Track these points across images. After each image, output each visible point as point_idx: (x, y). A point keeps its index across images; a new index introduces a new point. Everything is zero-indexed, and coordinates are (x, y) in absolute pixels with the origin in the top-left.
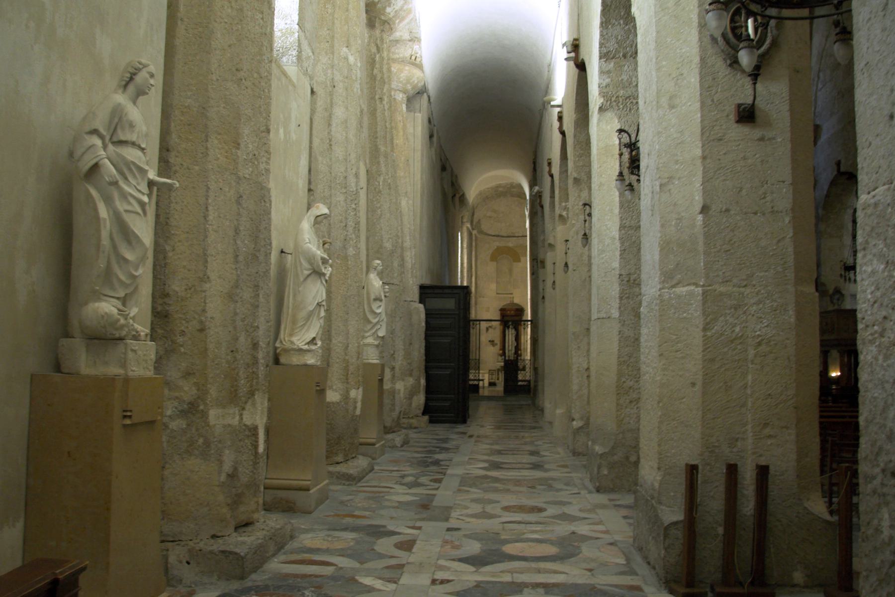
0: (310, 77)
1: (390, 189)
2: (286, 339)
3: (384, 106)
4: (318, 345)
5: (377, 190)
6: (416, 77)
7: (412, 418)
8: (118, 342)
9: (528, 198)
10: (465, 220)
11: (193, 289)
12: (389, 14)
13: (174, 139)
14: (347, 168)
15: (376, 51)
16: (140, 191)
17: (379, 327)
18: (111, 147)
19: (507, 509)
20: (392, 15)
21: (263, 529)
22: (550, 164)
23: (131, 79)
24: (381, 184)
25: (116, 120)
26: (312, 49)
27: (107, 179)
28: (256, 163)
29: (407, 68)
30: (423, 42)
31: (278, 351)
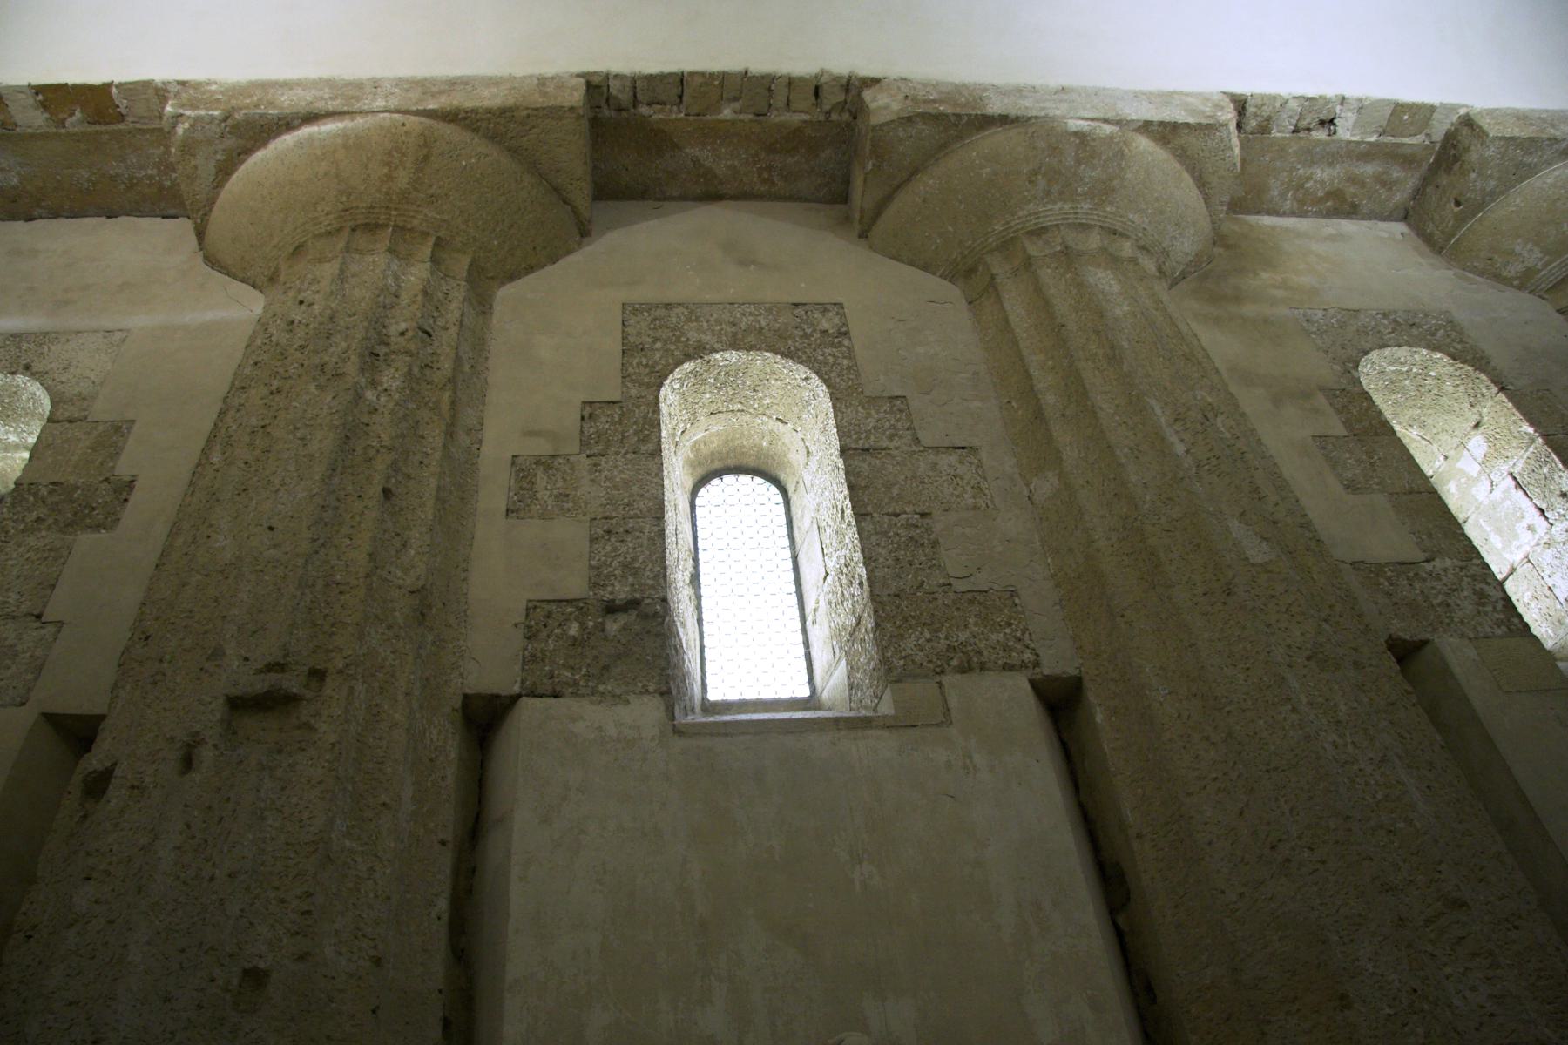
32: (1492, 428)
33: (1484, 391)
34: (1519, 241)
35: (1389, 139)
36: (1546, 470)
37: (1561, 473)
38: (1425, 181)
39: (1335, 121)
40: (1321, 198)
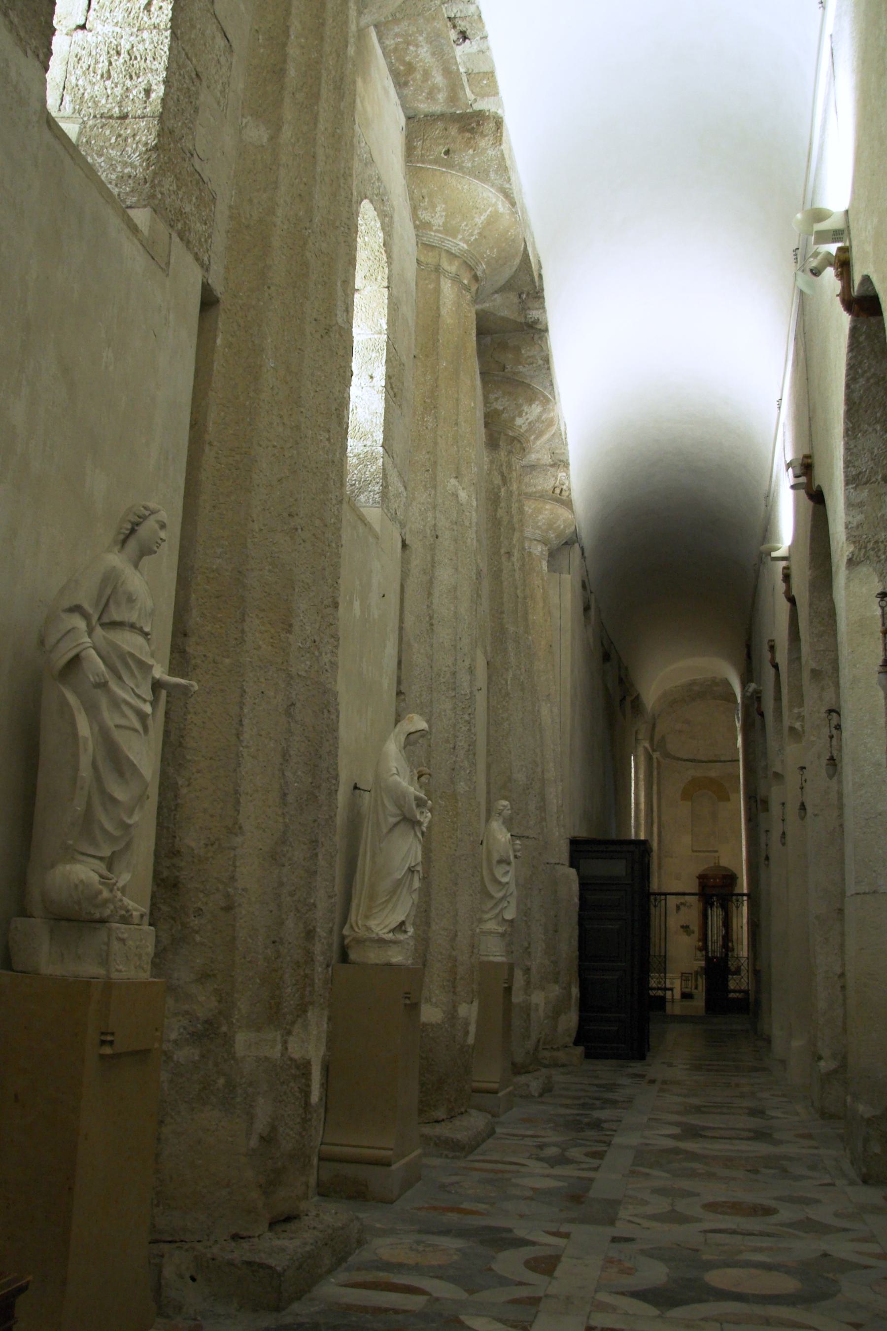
0: (400, 523)
1: (523, 690)
2: (360, 923)
3: (513, 565)
4: (410, 934)
5: (503, 691)
6: (562, 519)
7: (558, 1049)
8: (98, 925)
9: (739, 700)
10: (640, 737)
11: (216, 846)
12: (520, 427)
13: (194, 617)
14: (456, 659)
15: (500, 483)
16: (139, 696)
17: (506, 904)
18: (99, 631)
19: (712, 1207)
20: (524, 428)
21: (314, 1228)
22: (772, 648)
23: (133, 531)
24: (509, 682)
25: (108, 591)
26: (404, 482)
27: (92, 679)
28: (317, 653)
29: (548, 507)
30: (571, 467)
31: (347, 941)
32: (365, 301)
33: (379, 278)
34: (443, 206)
35: (464, 78)
36: (374, 355)
37: (380, 365)
38: (442, 116)
39: (467, 41)
40: (404, 61)
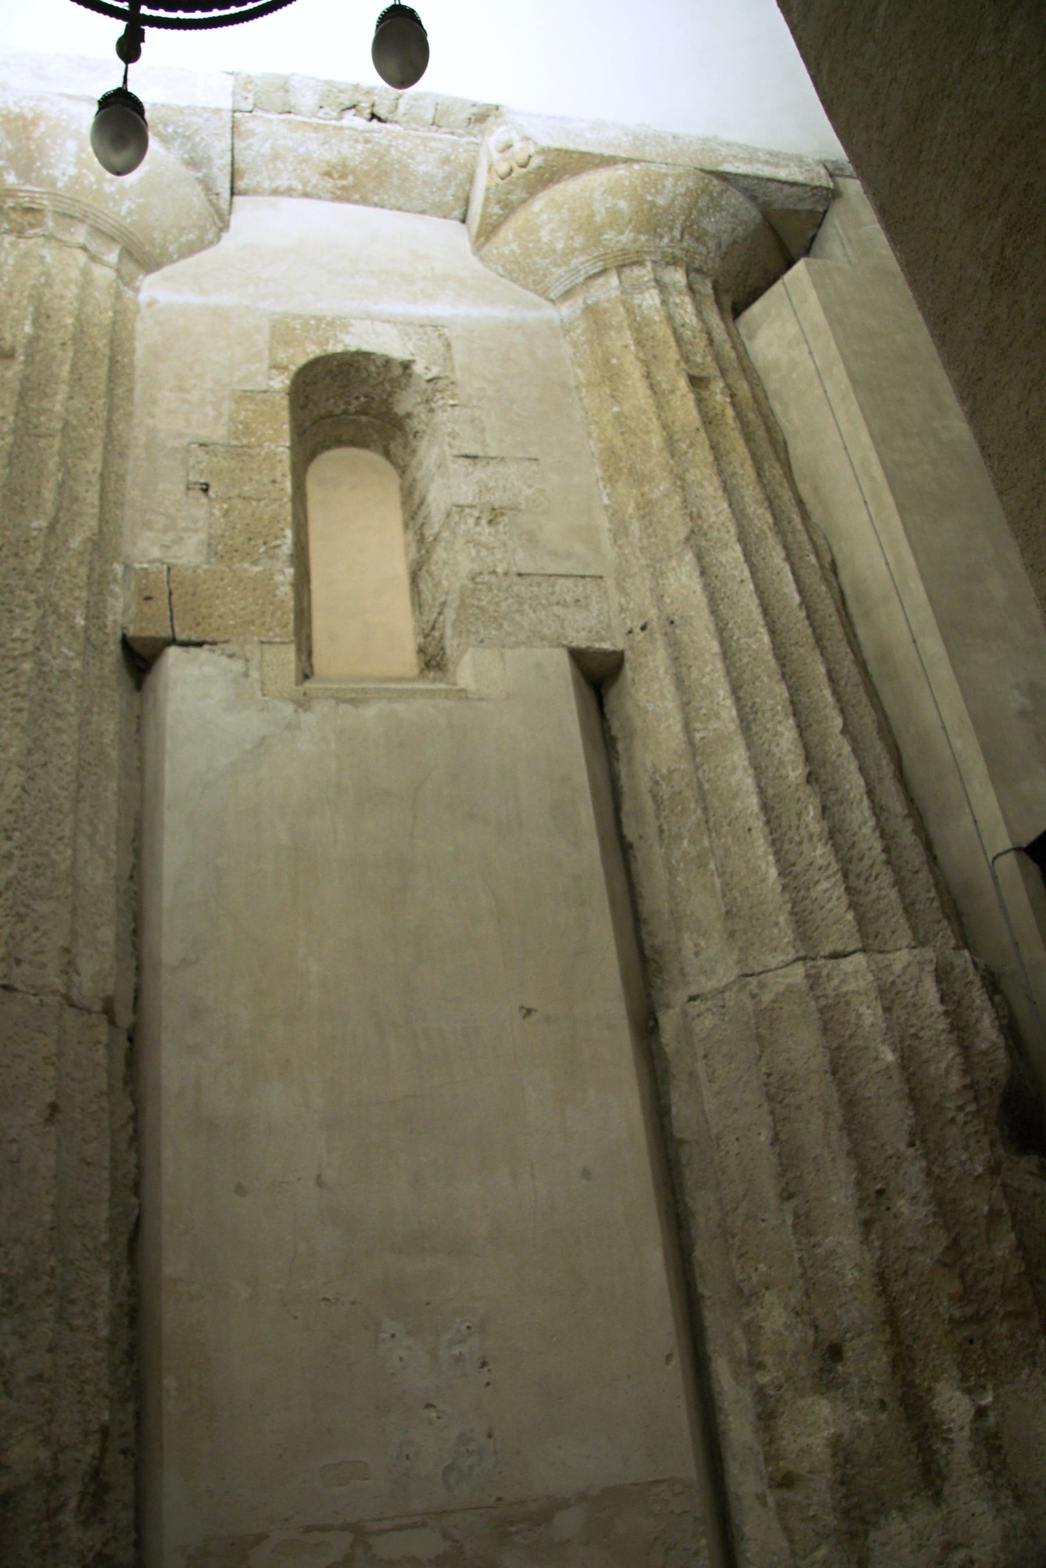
6: (597, 195)
